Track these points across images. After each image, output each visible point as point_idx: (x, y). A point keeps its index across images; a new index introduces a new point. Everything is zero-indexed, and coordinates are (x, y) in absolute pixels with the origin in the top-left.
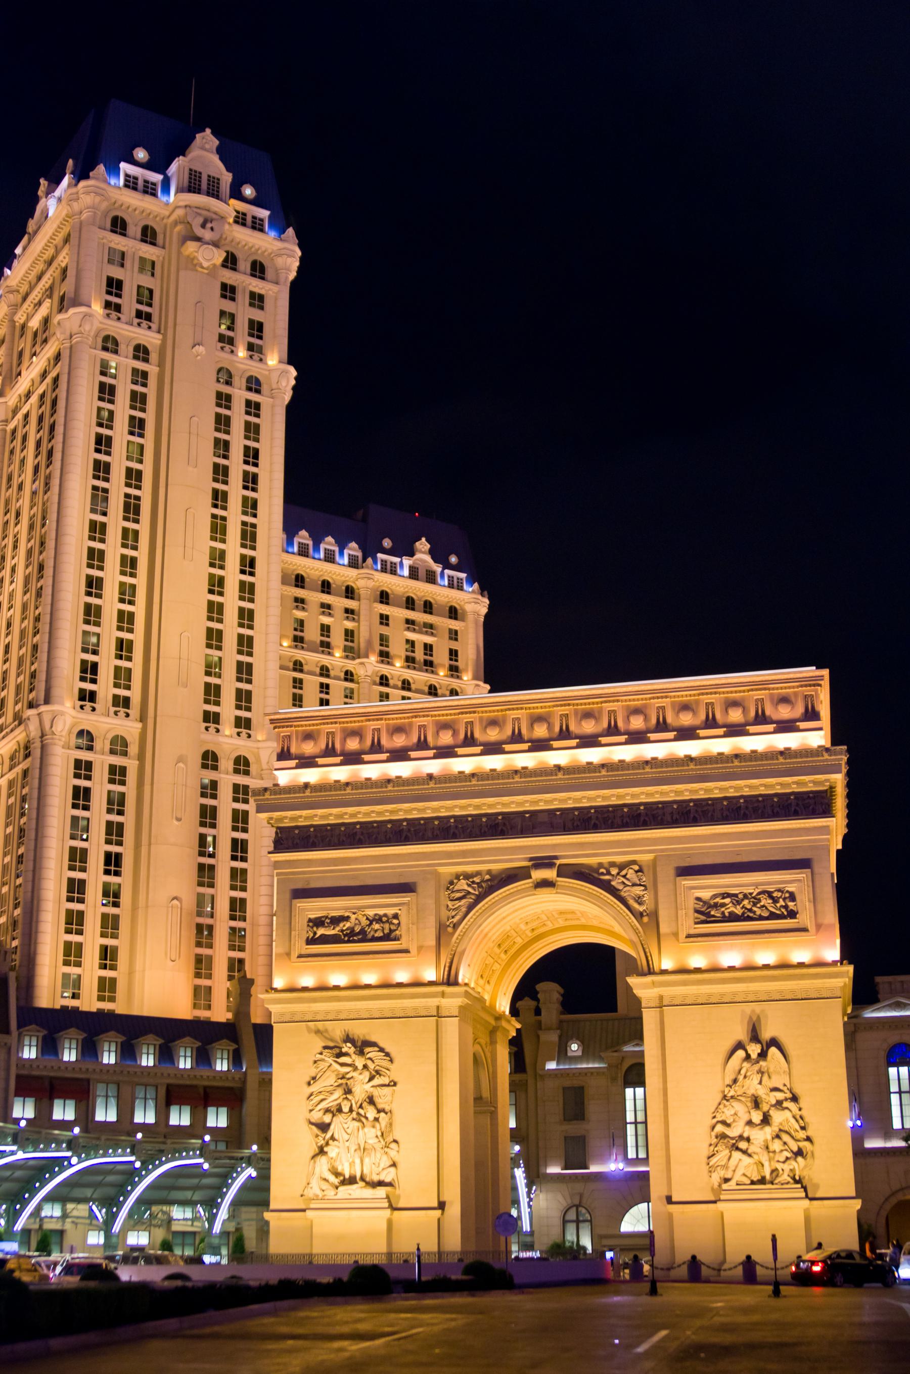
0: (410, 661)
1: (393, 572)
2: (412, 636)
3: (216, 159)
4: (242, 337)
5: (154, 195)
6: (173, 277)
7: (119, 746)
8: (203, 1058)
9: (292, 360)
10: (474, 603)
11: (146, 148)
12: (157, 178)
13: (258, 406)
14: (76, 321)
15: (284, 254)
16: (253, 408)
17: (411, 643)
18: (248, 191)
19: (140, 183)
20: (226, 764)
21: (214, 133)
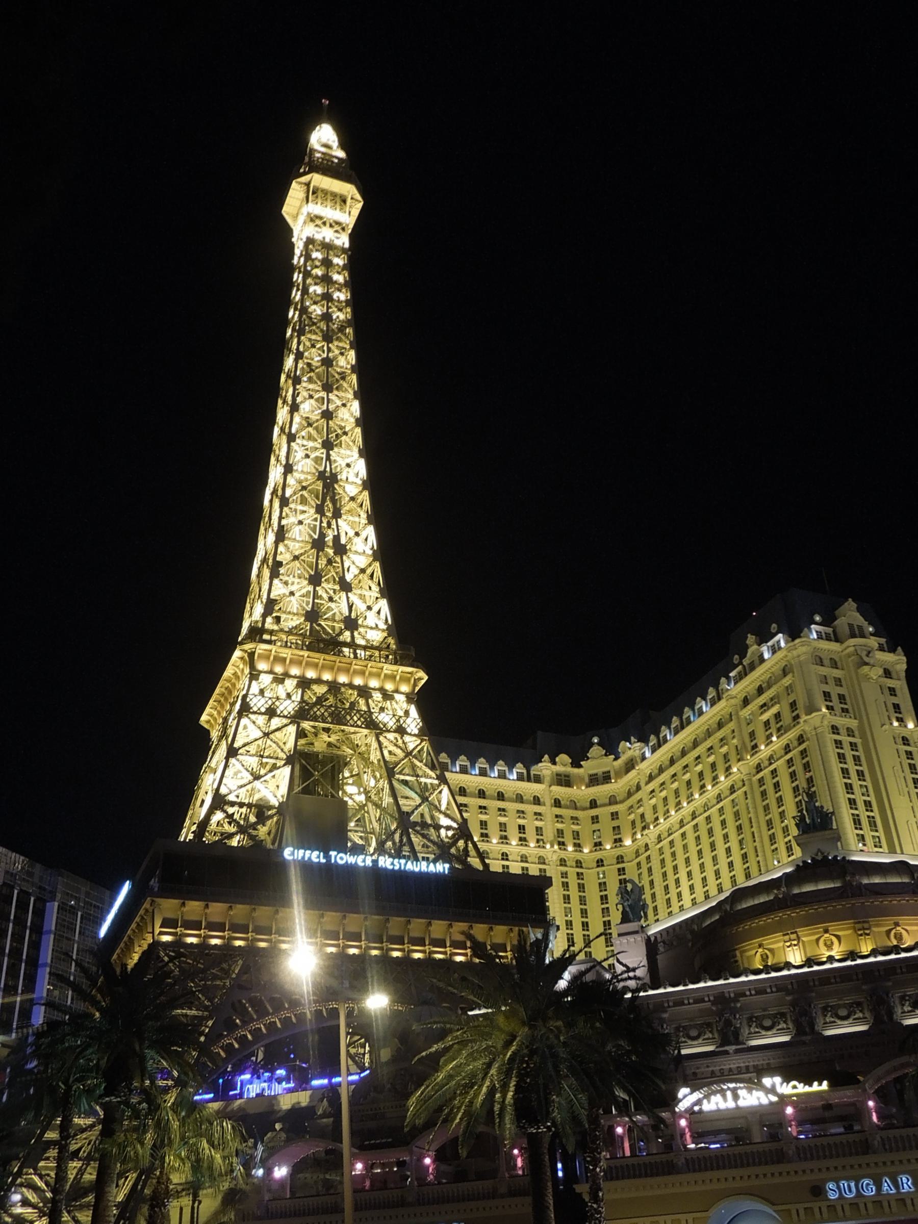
3: (858, 615)
11: (821, 616)
13: (911, 753)
15: (898, 661)
21: (854, 601)
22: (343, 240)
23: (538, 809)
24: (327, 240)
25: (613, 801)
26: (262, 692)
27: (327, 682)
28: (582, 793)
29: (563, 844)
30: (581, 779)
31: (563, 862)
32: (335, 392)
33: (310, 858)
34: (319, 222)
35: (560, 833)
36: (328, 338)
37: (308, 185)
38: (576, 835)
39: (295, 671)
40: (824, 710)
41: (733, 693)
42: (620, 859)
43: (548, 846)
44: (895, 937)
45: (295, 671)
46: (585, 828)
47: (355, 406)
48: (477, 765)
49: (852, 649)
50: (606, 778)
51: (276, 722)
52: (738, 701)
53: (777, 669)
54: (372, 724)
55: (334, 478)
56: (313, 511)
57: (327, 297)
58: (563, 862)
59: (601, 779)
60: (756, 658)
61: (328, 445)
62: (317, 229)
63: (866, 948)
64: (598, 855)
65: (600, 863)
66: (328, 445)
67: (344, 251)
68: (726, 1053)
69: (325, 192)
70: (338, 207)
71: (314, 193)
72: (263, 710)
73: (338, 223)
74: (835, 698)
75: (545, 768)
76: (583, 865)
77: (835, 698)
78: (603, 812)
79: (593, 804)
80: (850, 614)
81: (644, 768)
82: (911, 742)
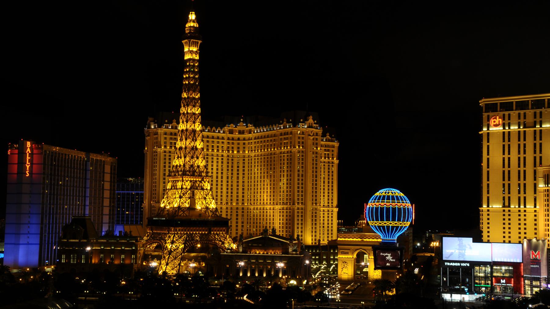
0: (325, 158)
7: (302, 209)
10: (336, 144)
22: (197, 58)
23: (223, 141)
25: (244, 139)
28: (236, 135)
30: (236, 131)
31: (228, 156)
38: (233, 148)
46: (235, 146)
53: (289, 131)
54: (203, 189)
57: (194, 77)
63: (265, 253)
66: (194, 123)
67: (197, 60)
74: (301, 143)
75: (226, 129)
77: (301, 143)
78: (241, 142)
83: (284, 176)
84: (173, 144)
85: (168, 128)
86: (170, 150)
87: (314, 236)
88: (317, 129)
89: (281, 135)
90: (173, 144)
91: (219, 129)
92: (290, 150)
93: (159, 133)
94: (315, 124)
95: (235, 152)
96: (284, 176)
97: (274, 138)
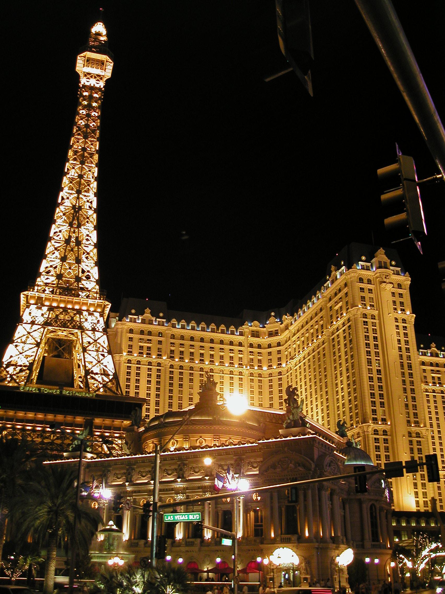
0: (434, 383)
1: (425, 355)
2: (433, 375)
3: (385, 256)
4: (399, 307)
5: (369, 270)
6: (379, 293)
8: (428, 523)
9: (413, 312)
12: (369, 264)
14: (356, 311)
15: (406, 280)
16: (405, 328)
17: (433, 378)
18: (393, 263)
19: (365, 267)
20: (414, 435)
22: (101, 84)
24: (92, 85)
25: (279, 344)
26: (30, 313)
27: (62, 308)
29: (253, 366)
30: (265, 333)
31: (252, 375)
32: (86, 164)
33: (31, 391)
34: (88, 76)
35: (252, 360)
36: (86, 137)
37: (85, 57)
38: (260, 361)
39: (47, 303)
40: (360, 306)
41: (325, 295)
42: (280, 373)
43: (244, 367)
44: (199, 442)
45: (47, 303)
46: (264, 358)
47: (96, 171)
48: (210, 327)
49: (378, 274)
50: (276, 333)
51: (35, 327)
52: (327, 299)
55: (80, 208)
56: (67, 225)
57: (88, 115)
58: (252, 375)
59: (274, 333)
60: (334, 278)
61: (79, 192)
62: (88, 80)
63: (186, 446)
64: (270, 371)
65: (270, 375)
66: (79, 192)
67: (100, 89)
68: (205, 479)
69: (94, 60)
70: (99, 67)
71: (88, 61)
72: (29, 322)
73: (99, 76)
74: (367, 299)
76: (262, 376)
79: (270, 346)
80: (381, 255)
81: (292, 328)
82: (407, 322)
83: (341, 374)
84: (145, 349)
85: (135, 322)
86: (139, 359)
87: (420, 495)
88: (398, 274)
89: (330, 299)
90: (145, 349)
91: (232, 328)
92: (347, 317)
93: (119, 330)
94: (391, 265)
95: (265, 368)
96: (341, 374)
97: (320, 315)
